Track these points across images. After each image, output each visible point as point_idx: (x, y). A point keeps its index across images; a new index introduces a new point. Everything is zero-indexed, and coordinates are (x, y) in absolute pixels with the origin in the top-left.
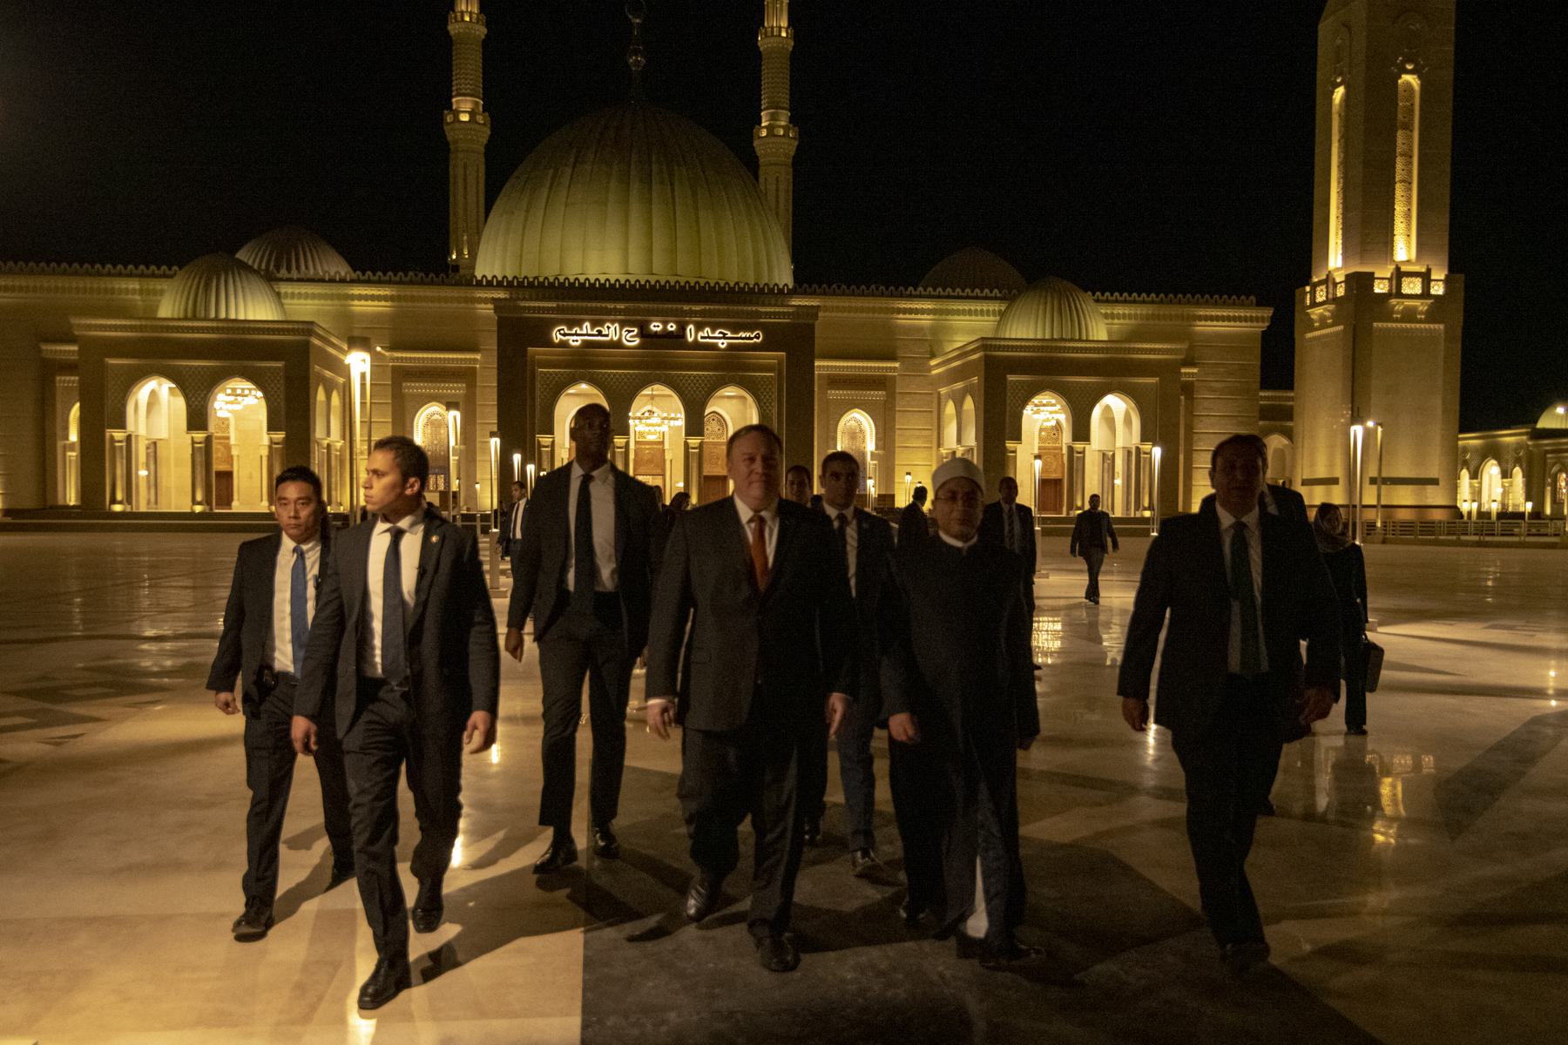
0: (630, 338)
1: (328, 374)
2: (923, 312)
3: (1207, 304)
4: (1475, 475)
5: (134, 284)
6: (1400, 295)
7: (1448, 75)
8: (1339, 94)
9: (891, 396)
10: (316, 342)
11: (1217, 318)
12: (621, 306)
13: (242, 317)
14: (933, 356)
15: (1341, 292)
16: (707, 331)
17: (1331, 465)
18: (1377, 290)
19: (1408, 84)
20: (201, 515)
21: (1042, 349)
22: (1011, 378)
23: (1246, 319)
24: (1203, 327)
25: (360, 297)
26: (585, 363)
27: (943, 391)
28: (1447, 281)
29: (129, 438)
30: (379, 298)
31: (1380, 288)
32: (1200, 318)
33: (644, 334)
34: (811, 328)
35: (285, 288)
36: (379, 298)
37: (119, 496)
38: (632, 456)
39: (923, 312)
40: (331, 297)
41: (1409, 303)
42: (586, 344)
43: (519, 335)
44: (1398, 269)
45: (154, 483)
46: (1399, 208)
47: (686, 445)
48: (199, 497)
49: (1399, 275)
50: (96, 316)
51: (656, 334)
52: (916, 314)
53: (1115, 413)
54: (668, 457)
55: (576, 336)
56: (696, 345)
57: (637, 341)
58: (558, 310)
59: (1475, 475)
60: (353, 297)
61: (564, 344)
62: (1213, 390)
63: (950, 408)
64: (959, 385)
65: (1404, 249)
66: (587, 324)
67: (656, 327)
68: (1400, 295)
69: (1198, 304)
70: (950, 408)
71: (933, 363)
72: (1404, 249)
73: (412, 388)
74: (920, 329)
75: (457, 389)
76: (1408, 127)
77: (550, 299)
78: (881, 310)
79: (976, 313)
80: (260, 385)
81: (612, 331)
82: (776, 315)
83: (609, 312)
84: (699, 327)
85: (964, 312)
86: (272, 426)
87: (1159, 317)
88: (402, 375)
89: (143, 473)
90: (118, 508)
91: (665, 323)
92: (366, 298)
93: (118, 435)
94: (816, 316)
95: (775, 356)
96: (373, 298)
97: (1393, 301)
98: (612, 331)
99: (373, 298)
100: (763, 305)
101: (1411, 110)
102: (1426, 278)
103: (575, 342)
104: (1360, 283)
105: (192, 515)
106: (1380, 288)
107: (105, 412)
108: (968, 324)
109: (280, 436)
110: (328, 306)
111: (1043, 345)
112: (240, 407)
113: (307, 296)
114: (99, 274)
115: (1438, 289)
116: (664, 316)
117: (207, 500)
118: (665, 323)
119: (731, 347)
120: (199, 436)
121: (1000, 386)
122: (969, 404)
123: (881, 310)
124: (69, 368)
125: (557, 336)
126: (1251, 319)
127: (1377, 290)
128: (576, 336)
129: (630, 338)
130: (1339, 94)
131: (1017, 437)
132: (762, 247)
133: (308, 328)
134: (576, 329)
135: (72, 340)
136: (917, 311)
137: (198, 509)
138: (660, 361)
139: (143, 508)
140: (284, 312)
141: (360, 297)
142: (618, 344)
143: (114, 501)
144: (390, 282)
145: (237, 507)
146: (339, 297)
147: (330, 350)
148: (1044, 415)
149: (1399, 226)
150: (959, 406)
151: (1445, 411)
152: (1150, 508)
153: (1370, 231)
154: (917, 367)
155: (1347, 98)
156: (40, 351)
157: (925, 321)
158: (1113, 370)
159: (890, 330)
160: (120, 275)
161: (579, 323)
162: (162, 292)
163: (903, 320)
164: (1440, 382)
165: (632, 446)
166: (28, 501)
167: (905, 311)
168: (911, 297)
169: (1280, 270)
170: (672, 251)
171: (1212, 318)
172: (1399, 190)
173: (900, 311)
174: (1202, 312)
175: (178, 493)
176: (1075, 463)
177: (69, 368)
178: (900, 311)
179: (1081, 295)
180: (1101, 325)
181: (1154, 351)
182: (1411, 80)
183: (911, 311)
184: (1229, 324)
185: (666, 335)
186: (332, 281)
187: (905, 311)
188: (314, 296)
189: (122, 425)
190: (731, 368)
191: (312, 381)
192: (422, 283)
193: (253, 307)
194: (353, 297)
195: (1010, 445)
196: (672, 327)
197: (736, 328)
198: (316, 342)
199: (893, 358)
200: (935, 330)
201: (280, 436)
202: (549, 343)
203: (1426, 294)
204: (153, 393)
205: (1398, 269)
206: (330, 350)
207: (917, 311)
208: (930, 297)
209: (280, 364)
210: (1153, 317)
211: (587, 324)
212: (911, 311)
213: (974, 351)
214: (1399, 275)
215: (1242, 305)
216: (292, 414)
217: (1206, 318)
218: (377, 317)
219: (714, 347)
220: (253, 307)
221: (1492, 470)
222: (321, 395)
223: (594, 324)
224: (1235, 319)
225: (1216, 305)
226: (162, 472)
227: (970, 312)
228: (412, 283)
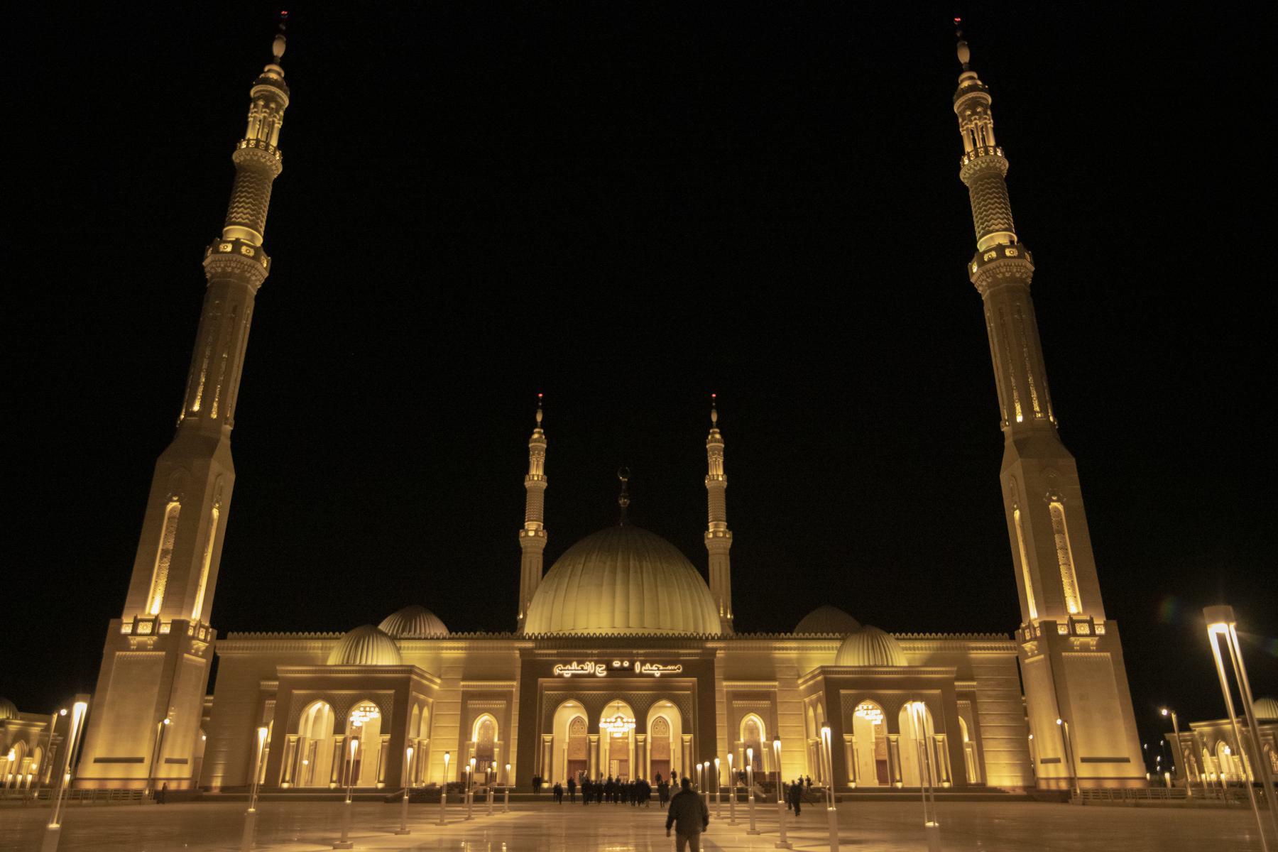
0: (601, 671)
1: (422, 697)
2: (791, 649)
3: (976, 640)
4: (1213, 753)
5: (318, 644)
6: (1075, 634)
7: (1079, 502)
8: (1017, 514)
9: (774, 704)
10: (415, 677)
11: (984, 649)
12: (595, 651)
13: (369, 663)
14: (799, 677)
15: (1038, 633)
16: (648, 666)
17: (1055, 749)
18: (1060, 632)
19: (1056, 508)
20: (335, 790)
21: (861, 672)
22: (843, 692)
23: (1003, 649)
24: (975, 655)
25: (447, 648)
26: (573, 689)
27: (807, 700)
28: (1105, 625)
29: (299, 740)
30: (458, 649)
31: (1062, 631)
32: (973, 649)
33: (610, 669)
34: (712, 662)
35: (404, 644)
36: (458, 649)
37: (287, 778)
38: (649, 747)
39: (791, 649)
40: (430, 648)
41: (1082, 639)
42: (574, 676)
43: (534, 670)
44: (1071, 619)
45: (312, 768)
46: (1065, 581)
47: (683, 741)
48: (335, 778)
49: (1072, 623)
50: (292, 665)
51: (617, 669)
52: (787, 650)
53: (915, 713)
54: (672, 747)
55: (567, 671)
56: (641, 675)
57: (605, 673)
58: (558, 655)
59: (1213, 753)
60: (442, 648)
61: (560, 676)
62: (989, 697)
63: (811, 713)
64: (814, 697)
65: (1074, 606)
66: (575, 664)
67: (616, 664)
68: (1075, 634)
69: (970, 639)
70: (811, 713)
71: (800, 681)
72: (1074, 606)
73: (474, 704)
74: (789, 660)
75: (500, 704)
76: (1061, 532)
77: (552, 648)
78: (764, 649)
79: (825, 649)
80: (379, 705)
81: (589, 667)
82: (689, 655)
83: (587, 655)
84: (643, 664)
85: (817, 649)
86: (383, 731)
87: (945, 649)
88: (468, 696)
89: (305, 762)
90: (285, 785)
91: (622, 662)
92: (450, 649)
93: (293, 738)
94: (714, 655)
95: (690, 681)
96: (454, 648)
97: (1072, 639)
98: (589, 667)
99: (454, 648)
100: (683, 648)
101: (1060, 523)
102: (1091, 624)
103: (567, 674)
104: (1049, 627)
105: (328, 790)
106: (1062, 631)
107: (286, 723)
108: (818, 655)
109: (387, 737)
110: (428, 654)
111: (862, 670)
112: (366, 717)
113: (416, 648)
114: (300, 639)
115: (1100, 631)
116: (622, 657)
117: (339, 780)
118: (622, 662)
119: (663, 676)
120: (340, 738)
121: (837, 697)
122: (820, 710)
123: (764, 649)
124: (272, 695)
125: (557, 671)
126: (1007, 649)
127: (1060, 632)
128: (567, 671)
129: (601, 671)
130: (1017, 514)
131: (851, 731)
132: (699, 611)
133: (410, 670)
134: (568, 667)
135: (276, 679)
136: (787, 649)
137: (333, 786)
138: (619, 686)
139: (302, 785)
140: (401, 658)
141: (447, 648)
142: (593, 675)
143: (284, 781)
144: (466, 639)
145: (361, 784)
146: (434, 648)
147: (425, 682)
148: (868, 716)
149: (1068, 592)
150: (815, 710)
151: (1123, 710)
152: (948, 780)
153: (1051, 596)
154: (790, 685)
155: (1021, 515)
156: (259, 685)
157: (793, 655)
158: (910, 685)
159: (771, 661)
160: (312, 639)
161: (570, 663)
162: (331, 648)
163: (779, 655)
164: (1116, 691)
165: (649, 740)
166: (236, 781)
167: (780, 649)
168: (783, 639)
169: (1005, 619)
170: (641, 613)
171: (980, 649)
172: (1063, 570)
173: (776, 649)
174: (973, 645)
175: (324, 778)
176: (892, 749)
177: (272, 695)
178: (776, 649)
179: (886, 636)
180: (903, 654)
181: (938, 672)
182: (1056, 505)
183: (783, 649)
184: (985, 651)
185: (622, 669)
186: (432, 639)
187: (780, 649)
188: (420, 648)
189: (295, 731)
190: (663, 689)
191: (410, 702)
192: (484, 639)
193: (381, 656)
194: (442, 648)
195: (847, 737)
196: (626, 664)
197: (665, 664)
198: (415, 677)
199: (774, 679)
200: (799, 660)
201: (387, 737)
202: (551, 675)
203: (1093, 634)
204: (319, 711)
205: (1071, 619)
206: (425, 682)
207: (787, 649)
208: (795, 639)
209: (392, 692)
210: (941, 649)
211: (575, 664)
212: (783, 649)
213: (819, 674)
214: (1072, 623)
215: (1001, 640)
216: (396, 725)
217: (977, 649)
218: (456, 660)
219: (652, 676)
220: (381, 656)
221: (1225, 750)
222: (416, 710)
223: (579, 663)
224: (996, 649)
225: (982, 640)
226: (318, 761)
227: (821, 649)
228: (478, 639)
